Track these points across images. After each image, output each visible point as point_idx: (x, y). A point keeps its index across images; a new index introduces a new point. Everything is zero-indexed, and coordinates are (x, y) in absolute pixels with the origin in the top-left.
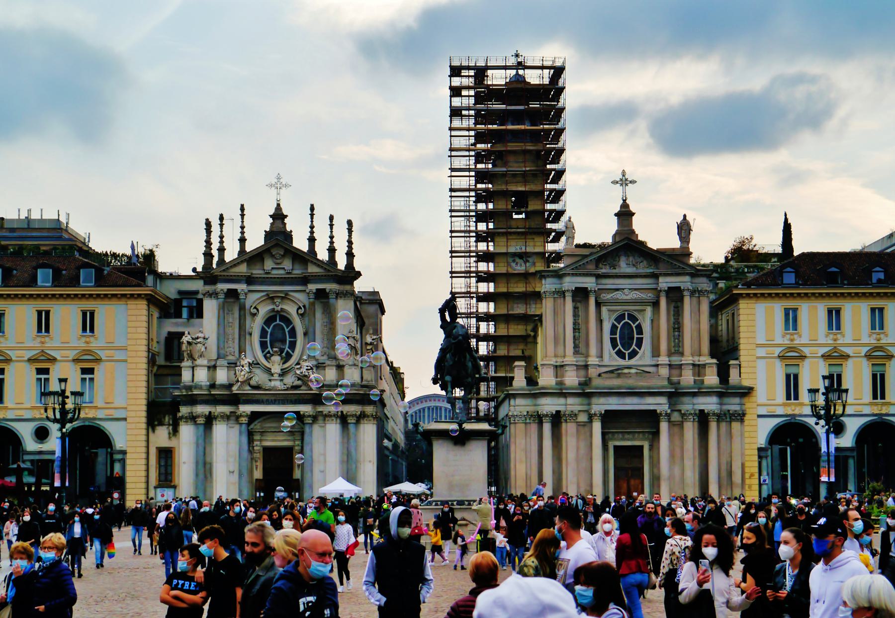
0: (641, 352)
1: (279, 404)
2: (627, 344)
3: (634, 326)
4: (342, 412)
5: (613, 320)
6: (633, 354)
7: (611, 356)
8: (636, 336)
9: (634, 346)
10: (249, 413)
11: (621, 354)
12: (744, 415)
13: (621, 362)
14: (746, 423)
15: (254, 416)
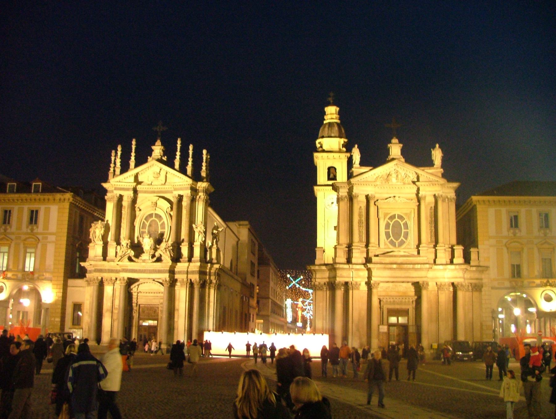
0: (407, 242)
1: (147, 273)
2: (397, 235)
3: (402, 223)
4: (191, 280)
5: (387, 219)
6: (402, 243)
7: (385, 244)
8: (403, 231)
9: (402, 238)
10: (126, 278)
11: (392, 243)
12: (482, 286)
13: (391, 248)
14: (483, 293)
15: (131, 282)
